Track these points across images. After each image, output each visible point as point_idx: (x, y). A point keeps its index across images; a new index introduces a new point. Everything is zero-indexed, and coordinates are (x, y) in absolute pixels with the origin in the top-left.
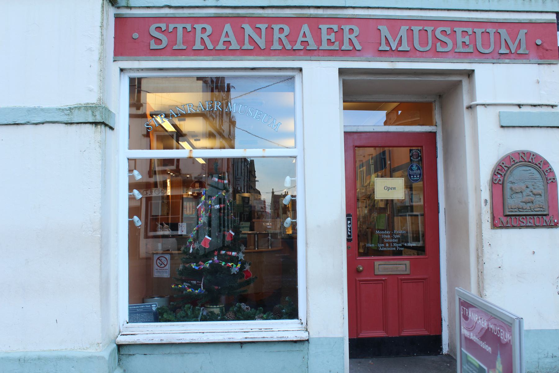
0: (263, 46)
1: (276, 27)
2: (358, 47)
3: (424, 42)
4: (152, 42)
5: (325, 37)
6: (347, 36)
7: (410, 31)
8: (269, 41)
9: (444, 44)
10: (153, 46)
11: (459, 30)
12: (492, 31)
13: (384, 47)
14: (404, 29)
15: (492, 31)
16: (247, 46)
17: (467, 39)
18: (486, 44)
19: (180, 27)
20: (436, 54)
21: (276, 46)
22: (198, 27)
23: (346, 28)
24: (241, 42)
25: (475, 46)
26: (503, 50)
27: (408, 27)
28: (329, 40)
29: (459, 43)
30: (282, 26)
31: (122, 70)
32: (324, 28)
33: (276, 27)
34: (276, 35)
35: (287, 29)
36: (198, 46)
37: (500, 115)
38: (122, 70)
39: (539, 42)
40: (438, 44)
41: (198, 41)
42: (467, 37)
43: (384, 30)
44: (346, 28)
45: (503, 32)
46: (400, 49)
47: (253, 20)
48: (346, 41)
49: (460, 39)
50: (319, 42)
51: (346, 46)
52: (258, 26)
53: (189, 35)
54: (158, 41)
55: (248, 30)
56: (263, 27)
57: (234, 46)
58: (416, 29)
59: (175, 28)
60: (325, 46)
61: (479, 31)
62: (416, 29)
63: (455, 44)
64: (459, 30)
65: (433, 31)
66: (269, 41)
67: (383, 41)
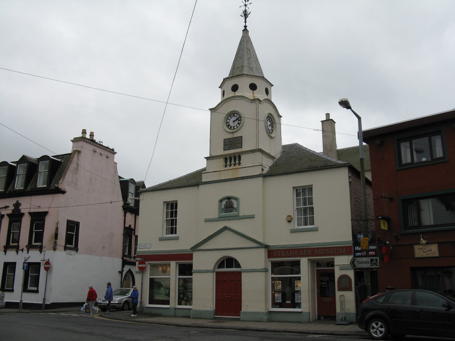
1: (296, 251)
7: (321, 251)
8: (295, 254)
9: (328, 253)
10: (274, 256)
11: (331, 249)
12: (338, 249)
13: (316, 254)
14: (320, 250)
15: (338, 249)
16: (291, 255)
18: (337, 252)
22: (282, 252)
24: (290, 254)
25: (334, 252)
26: (340, 253)
27: (320, 250)
28: (306, 253)
29: (331, 252)
30: (297, 251)
31: (269, 260)
32: (305, 251)
33: (296, 251)
34: (296, 253)
36: (282, 256)
37: (340, 267)
38: (269, 260)
40: (327, 253)
41: (282, 254)
42: (333, 251)
43: (316, 250)
45: (340, 249)
46: (319, 254)
47: (292, 250)
50: (303, 253)
51: (309, 254)
52: (293, 251)
53: (281, 253)
54: (275, 255)
55: (291, 252)
56: (293, 251)
57: (289, 255)
58: (322, 250)
59: (278, 252)
61: (335, 249)
63: (330, 252)
64: (331, 249)
65: (326, 250)
66: (295, 254)
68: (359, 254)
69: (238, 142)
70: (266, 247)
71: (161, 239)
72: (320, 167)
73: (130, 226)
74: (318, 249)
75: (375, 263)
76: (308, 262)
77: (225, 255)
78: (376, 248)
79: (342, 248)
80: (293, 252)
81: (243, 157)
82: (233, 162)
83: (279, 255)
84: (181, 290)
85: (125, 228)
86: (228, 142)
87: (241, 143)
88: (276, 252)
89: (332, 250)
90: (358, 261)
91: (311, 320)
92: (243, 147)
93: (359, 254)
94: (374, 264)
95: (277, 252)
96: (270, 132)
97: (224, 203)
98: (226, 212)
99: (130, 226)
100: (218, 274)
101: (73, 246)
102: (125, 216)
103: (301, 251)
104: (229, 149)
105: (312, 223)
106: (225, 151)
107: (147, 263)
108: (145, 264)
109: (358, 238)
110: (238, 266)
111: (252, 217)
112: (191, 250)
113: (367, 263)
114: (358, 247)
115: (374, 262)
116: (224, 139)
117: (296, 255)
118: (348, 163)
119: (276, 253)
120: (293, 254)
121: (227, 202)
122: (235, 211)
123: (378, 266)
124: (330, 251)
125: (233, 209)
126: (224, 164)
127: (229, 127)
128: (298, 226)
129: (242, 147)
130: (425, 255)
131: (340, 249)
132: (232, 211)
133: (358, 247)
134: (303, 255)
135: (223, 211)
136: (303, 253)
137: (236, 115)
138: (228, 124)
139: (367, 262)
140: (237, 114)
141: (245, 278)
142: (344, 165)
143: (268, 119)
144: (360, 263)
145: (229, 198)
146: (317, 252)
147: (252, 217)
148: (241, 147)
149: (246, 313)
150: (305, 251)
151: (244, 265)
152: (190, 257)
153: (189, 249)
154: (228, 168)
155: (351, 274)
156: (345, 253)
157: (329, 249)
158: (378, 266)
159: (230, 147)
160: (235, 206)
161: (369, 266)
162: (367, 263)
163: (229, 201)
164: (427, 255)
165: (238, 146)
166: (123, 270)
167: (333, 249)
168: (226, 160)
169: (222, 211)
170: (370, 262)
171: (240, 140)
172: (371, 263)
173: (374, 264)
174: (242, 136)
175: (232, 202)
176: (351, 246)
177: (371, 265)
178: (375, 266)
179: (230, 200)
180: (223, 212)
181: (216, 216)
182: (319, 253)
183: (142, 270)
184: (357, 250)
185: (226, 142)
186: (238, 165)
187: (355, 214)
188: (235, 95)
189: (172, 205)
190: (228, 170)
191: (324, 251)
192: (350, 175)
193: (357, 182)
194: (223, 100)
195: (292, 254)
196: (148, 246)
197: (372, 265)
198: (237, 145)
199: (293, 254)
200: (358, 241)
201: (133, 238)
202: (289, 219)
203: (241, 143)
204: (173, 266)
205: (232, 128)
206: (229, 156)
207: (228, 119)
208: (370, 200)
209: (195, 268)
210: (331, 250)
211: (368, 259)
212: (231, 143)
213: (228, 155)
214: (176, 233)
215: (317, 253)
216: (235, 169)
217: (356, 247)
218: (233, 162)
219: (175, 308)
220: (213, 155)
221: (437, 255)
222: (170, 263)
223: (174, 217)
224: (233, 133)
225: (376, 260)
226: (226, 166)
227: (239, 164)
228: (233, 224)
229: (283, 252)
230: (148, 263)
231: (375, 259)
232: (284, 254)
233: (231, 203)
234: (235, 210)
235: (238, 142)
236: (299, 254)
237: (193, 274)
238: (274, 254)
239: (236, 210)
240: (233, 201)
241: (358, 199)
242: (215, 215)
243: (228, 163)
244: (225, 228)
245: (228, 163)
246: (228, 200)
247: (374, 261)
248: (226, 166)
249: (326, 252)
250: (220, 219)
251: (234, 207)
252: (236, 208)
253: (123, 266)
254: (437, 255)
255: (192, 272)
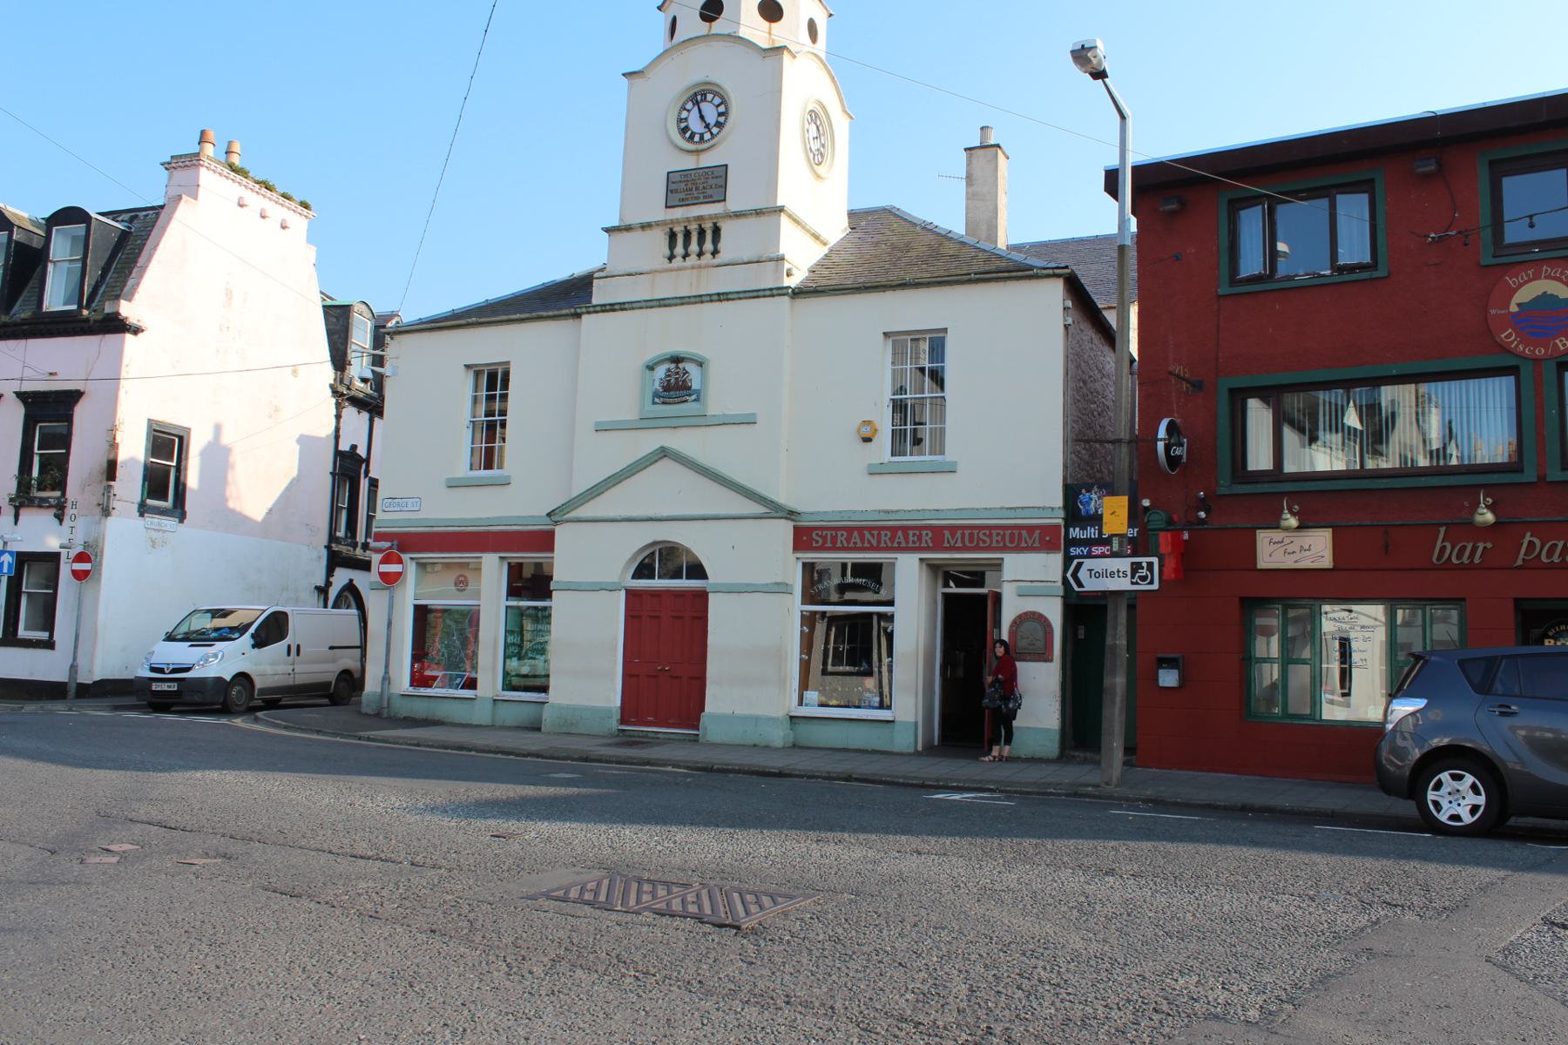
0: (875, 545)
1: (883, 533)
2: (931, 545)
3: (971, 541)
4: (814, 542)
5: (911, 538)
6: (924, 538)
7: (963, 535)
8: (879, 542)
9: (984, 542)
10: (814, 545)
11: (994, 532)
15: (1016, 532)
16: (866, 545)
17: (999, 538)
18: (1012, 541)
19: (829, 533)
20: (977, 549)
21: (883, 545)
23: (924, 533)
24: (863, 543)
26: (1023, 545)
29: (994, 542)
32: (911, 533)
33: (883, 533)
34: (883, 538)
35: (889, 534)
36: (839, 545)
39: (1048, 539)
40: (981, 542)
41: (839, 541)
44: (924, 533)
46: (956, 545)
47: (870, 529)
48: (924, 542)
49: (995, 538)
50: (907, 542)
51: (923, 545)
52: (873, 532)
53: (834, 539)
54: (817, 542)
55: (867, 534)
56: (875, 533)
58: (967, 532)
60: (911, 545)
61: (1008, 532)
62: (967, 532)
63: (991, 541)
64: (994, 532)
66: (879, 542)
67: (946, 541)
68: (1082, 551)
69: (713, 182)
70: (791, 514)
71: (453, 485)
72: (976, 274)
73: (354, 447)
74: (953, 529)
75: (1147, 575)
76: (921, 568)
77: (659, 539)
78: (1135, 535)
79: (1031, 529)
80: (873, 536)
81: (727, 228)
82: (694, 247)
83: (829, 544)
84: (513, 644)
85: (338, 453)
86: (681, 182)
87: (721, 186)
88: (820, 533)
89: (998, 534)
90: (1090, 570)
91: (920, 748)
92: (727, 198)
93: (1082, 551)
94: (1143, 578)
95: (824, 533)
96: (817, 162)
97: (661, 372)
98: (664, 403)
99: (354, 447)
100: (632, 595)
101: (169, 504)
102: (338, 417)
103: (900, 533)
104: (683, 204)
105: (939, 448)
106: (668, 210)
107: (405, 557)
108: (400, 561)
109: (1080, 502)
110: (697, 571)
111: (749, 421)
112: (548, 520)
113: (1121, 574)
114: (1077, 529)
115: (1144, 572)
116: (668, 173)
117: (883, 545)
118: (1066, 267)
119: (820, 536)
120: (874, 542)
121: (669, 370)
122: (695, 400)
123: (1155, 586)
124: (990, 536)
125: (690, 395)
126: (668, 252)
127: (688, 135)
128: (892, 455)
129: (725, 200)
130: (1288, 563)
131: (1024, 532)
132: (686, 401)
133: (1077, 529)
134: (903, 545)
135: (657, 400)
136: (907, 542)
137: (709, 97)
138: (683, 125)
139: (1118, 571)
140: (716, 94)
141: (719, 611)
142: (1050, 272)
143: (811, 117)
144: (1098, 575)
145: (677, 360)
146: (950, 537)
147: (749, 421)
148: (722, 198)
149: (719, 718)
150: (911, 533)
151: (715, 574)
152: (545, 541)
153: (545, 514)
154: (678, 261)
155: (1053, 611)
156: (1036, 545)
157: (987, 532)
158: (1155, 586)
159: (687, 199)
160: (695, 386)
161: (1124, 584)
162: (1121, 574)
163: (677, 368)
164: (1296, 562)
165: (711, 196)
166: (328, 584)
167: (1002, 532)
168: (672, 236)
169: (653, 400)
170: (1129, 573)
171: (721, 177)
172: (1133, 577)
173: (1143, 578)
174: (726, 166)
175: (687, 372)
176: (1057, 527)
177: (1132, 583)
178: (1143, 587)
179: (681, 365)
180: (654, 403)
181: (629, 413)
182: (956, 542)
183: (389, 579)
184: (1074, 539)
185: (673, 183)
186: (711, 256)
187: (1073, 427)
188: (712, 32)
189: (492, 377)
190: (679, 269)
191: (971, 535)
192: (1069, 304)
193: (1082, 331)
194: (669, 45)
195: (869, 542)
196: (410, 505)
197: (1137, 583)
198: (709, 192)
199: (874, 542)
200: (1080, 510)
201: (364, 485)
202: (866, 432)
203: (721, 186)
204: (492, 570)
205: (697, 138)
206: (683, 229)
207: (685, 109)
208: (1111, 392)
209: (560, 574)
210: (994, 535)
211: (1124, 564)
212: (690, 186)
213: (678, 221)
214: (500, 467)
215: (948, 542)
216: (700, 267)
217: (1071, 529)
218: (694, 247)
219: (495, 700)
220: (630, 221)
221: (1326, 562)
222: (481, 557)
223: (499, 416)
224: (697, 152)
225: (1150, 565)
226: (671, 258)
227: (715, 253)
228: (682, 441)
229: (842, 535)
230: (412, 559)
231: (1145, 565)
232: (845, 542)
233: (684, 374)
234: (693, 397)
235: (713, 182)
236: (892, 542)
237: (554, 594)
238: (813, 539)
239: (698, 396)
240: (690, 367)
241: (1081, 384)
242: (628, 411)
243: (679, 249)
244: (664, 453)
245: (679, 249)
246: (673, 366)
247: (1143, 568)
248: (671, 258)
249: (979, 539)
250: (645, 423)
251: (693, 388)
252: (698, 392)
253: (330, 572)
254: (1326, 562)
255: (551, 589)
